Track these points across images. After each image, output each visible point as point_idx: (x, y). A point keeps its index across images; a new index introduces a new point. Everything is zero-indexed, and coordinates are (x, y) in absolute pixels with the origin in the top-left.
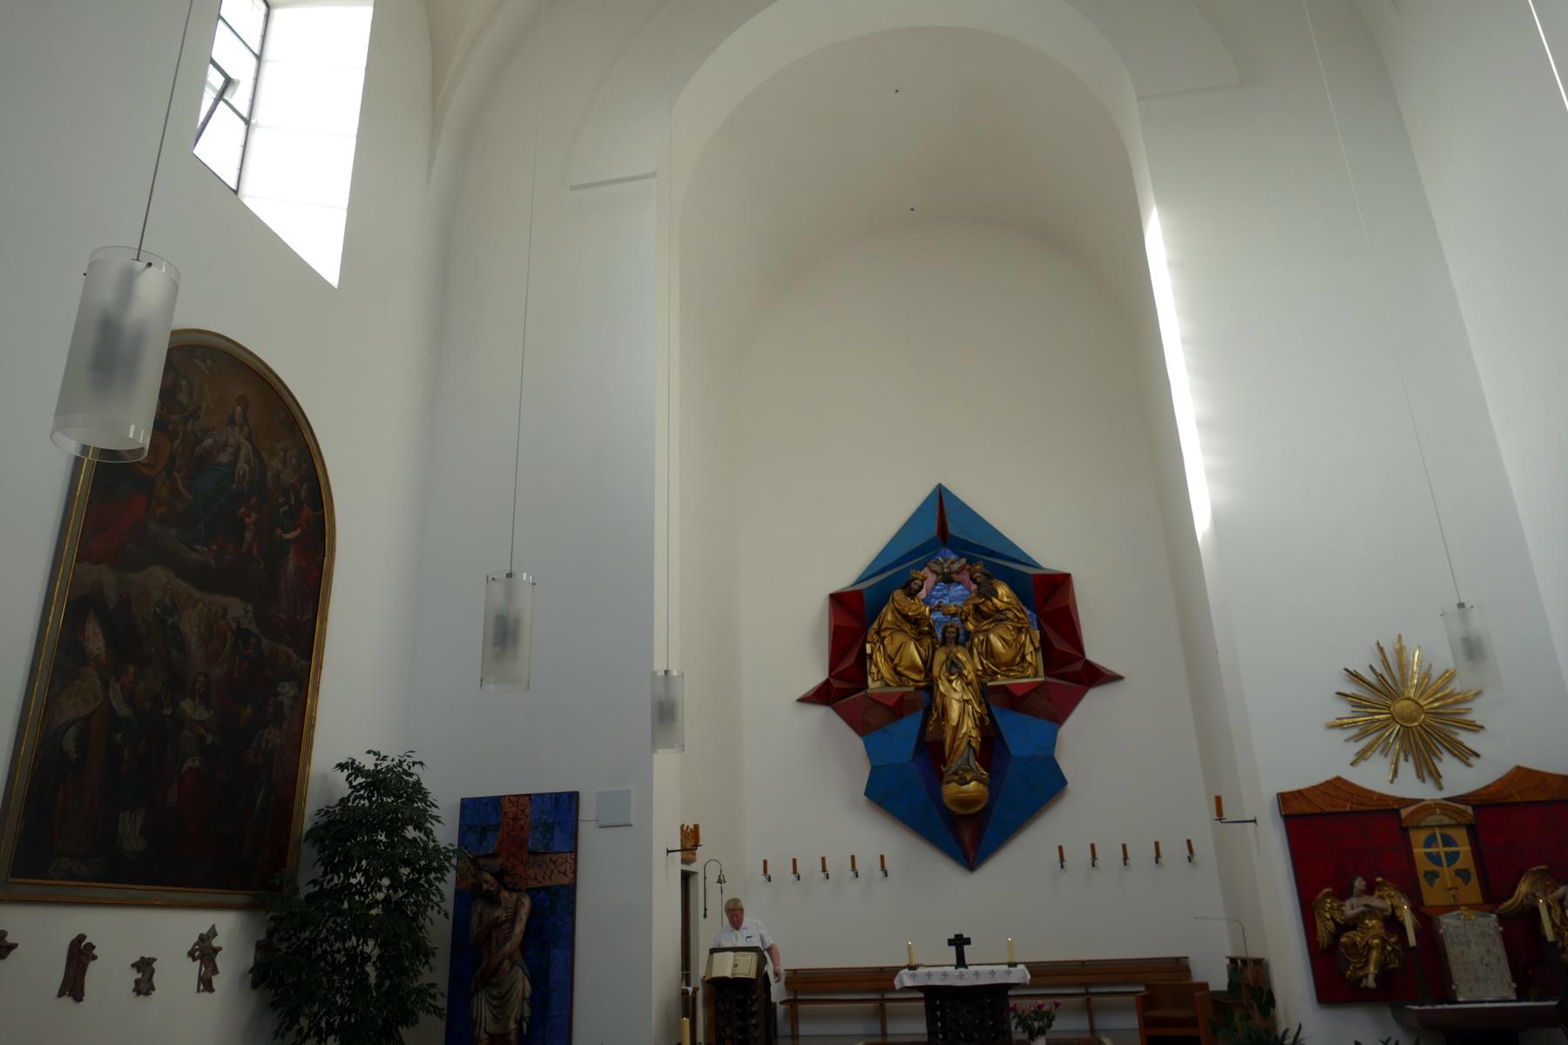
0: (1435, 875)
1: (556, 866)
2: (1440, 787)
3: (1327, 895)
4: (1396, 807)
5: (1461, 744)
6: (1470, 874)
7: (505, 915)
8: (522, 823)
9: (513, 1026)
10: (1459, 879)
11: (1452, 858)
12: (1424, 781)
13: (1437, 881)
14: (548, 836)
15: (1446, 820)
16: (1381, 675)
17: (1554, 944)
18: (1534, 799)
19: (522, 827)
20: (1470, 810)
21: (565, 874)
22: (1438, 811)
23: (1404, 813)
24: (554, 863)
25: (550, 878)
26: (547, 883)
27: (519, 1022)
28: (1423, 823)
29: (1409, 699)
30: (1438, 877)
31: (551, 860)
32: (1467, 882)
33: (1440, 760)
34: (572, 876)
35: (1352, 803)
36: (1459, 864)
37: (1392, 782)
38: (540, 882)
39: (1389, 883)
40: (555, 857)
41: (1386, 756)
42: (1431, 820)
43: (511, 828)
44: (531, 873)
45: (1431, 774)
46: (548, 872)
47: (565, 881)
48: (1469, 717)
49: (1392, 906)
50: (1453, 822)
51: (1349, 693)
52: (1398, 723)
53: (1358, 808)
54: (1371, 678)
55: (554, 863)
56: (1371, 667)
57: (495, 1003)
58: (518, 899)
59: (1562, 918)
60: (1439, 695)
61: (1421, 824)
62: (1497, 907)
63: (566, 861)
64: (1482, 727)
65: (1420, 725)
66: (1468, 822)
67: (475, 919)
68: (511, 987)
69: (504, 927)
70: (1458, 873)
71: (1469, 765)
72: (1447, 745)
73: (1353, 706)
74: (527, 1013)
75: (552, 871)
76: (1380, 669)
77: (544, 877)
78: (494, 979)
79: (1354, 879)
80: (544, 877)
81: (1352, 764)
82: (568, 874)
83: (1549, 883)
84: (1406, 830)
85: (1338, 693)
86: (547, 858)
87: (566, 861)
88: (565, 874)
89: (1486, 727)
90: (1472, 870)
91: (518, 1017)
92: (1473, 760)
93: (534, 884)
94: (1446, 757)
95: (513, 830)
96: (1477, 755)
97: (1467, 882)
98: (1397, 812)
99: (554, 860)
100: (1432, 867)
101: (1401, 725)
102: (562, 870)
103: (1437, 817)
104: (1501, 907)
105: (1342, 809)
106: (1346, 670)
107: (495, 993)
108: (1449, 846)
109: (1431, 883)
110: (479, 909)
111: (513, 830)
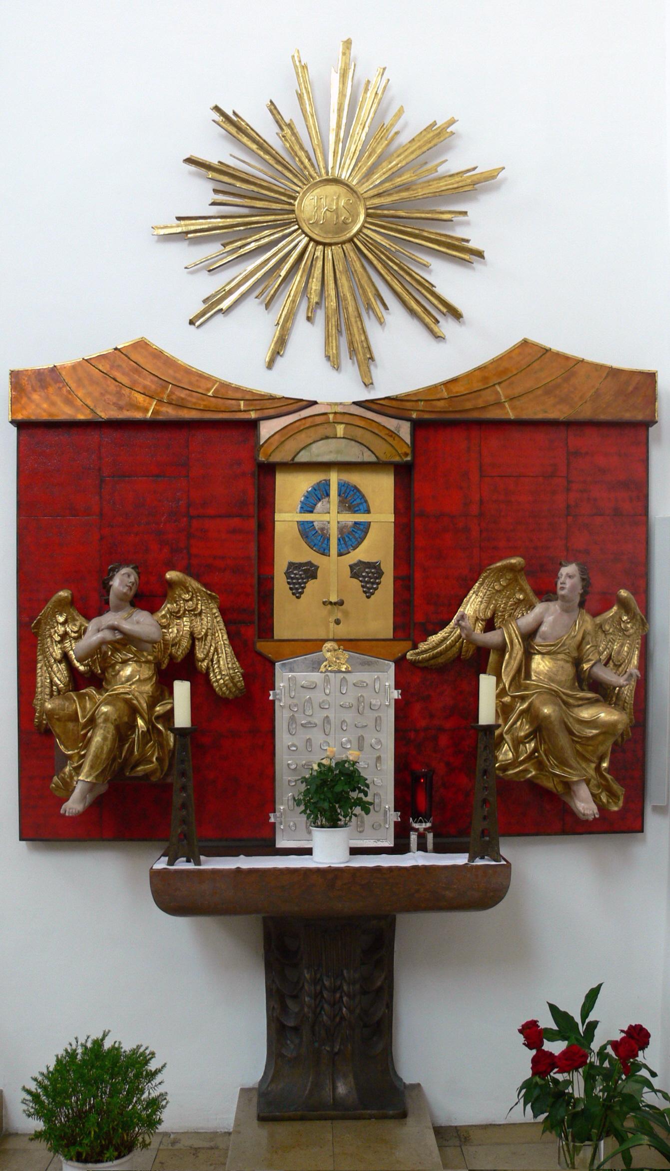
0: (310, 571)
2: (368, 384)
3: (61, 606)
4: (253, 415)
5: (429, 289)
6: (380, 574)
10: (356, 583)
11: (359, 531)
12: (337, 367)
13: (311, 585)
15: (354, 453)
16: (290, 126)
17: (489, 729)
18: (540, 416)
20: (405, 430)
22: (340, 430)
23: (267, 429)
28: (303, 457)
29: (336, 181)
30: (314, 576)
32: (369, 593)
33: (381, 322)
35: (160, 401)
36: (361, 554)
37: (270, 365)
39: (195, 584)
41: (267, 306)
42: (321, 451)
45: (353, 351)
48: (460, 232)
49: (193, 637)
50: (368, 457)
51: (213, 160)
52: (307, 235)
53: (170, 413)
54: (268, 131)
56: (273, 108)
59: (519, 671)
60: (398, 181)
61: (297, 460)
62: (415, 647)
64: (480, 254)
65: (351, 240)
66: (397, 459)
70: (357, 570)
71: (438, 337)
72: (399, 289)
73: (216, 191)
76: (289, 112)
79: (114, 570)
81: (192, 322)
83: (521, 597)
84: (268, 470)
85: (190, 161)
89: (485, 255)
90: (388, 568)
92: (447, 326)
94: (396, 315)
96: (456, 314)
97: (369, 593)
98: (253, 425)
100: (307, 555)
101: (311, 239)
103: (332, 444)
104: (423, 646)
105: (139, 415)
106: (217, 109)
108: (353, 509)
109: (297, 590)
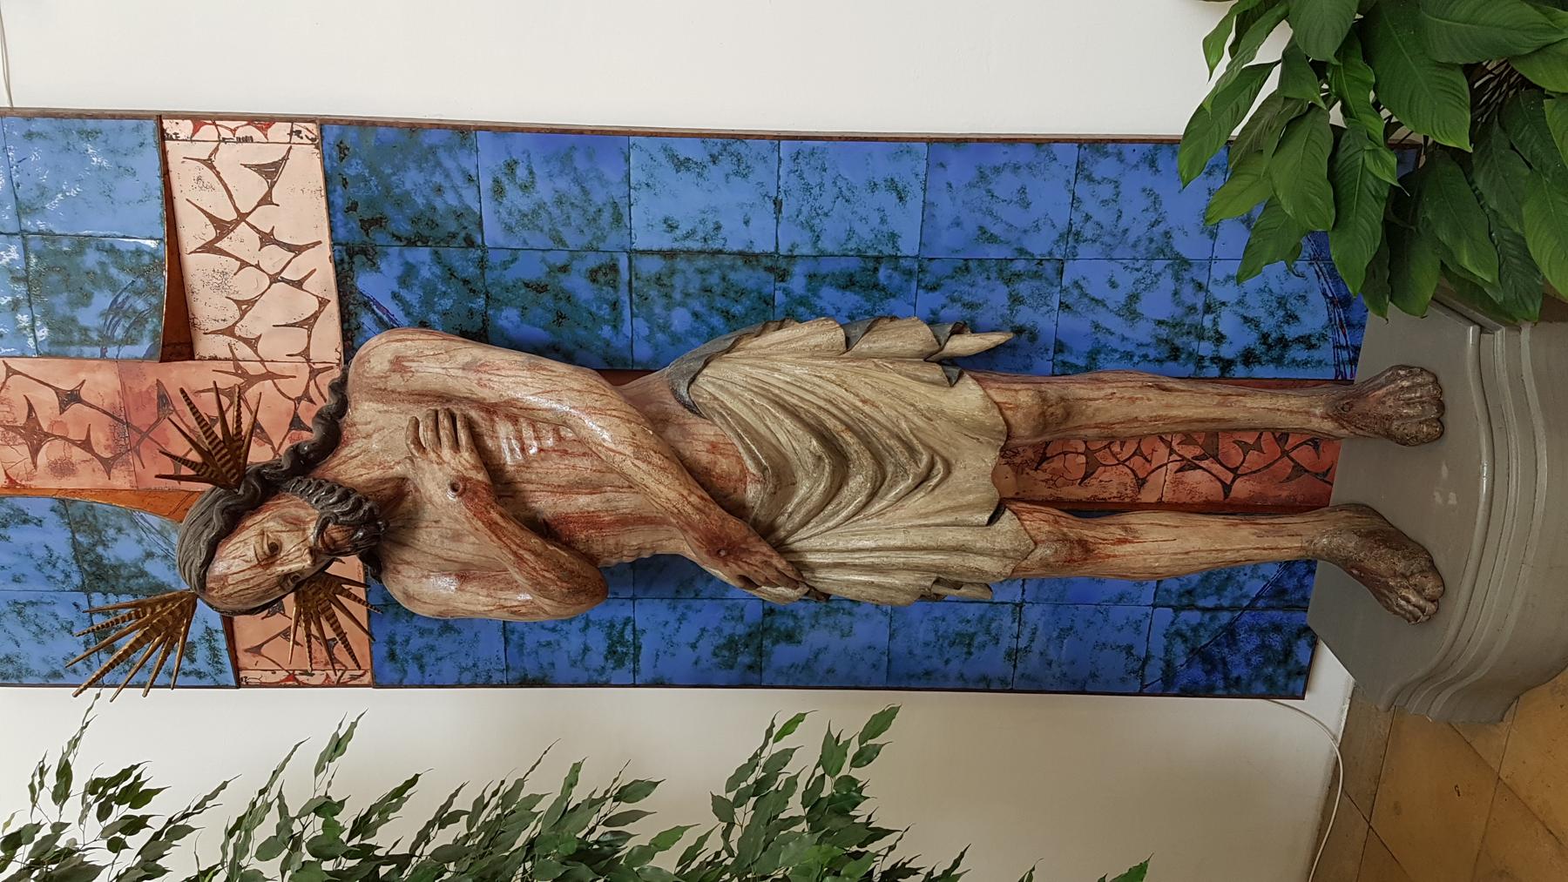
1: (242, 217)
7: (446, 453)
8: (46, 402)
9: (968, 397)
14: (91, 259)
19: (70, 398)
21: (271, 172)
24: (223, 228)
25: (297, 250)
26: (320, 266)
27: (956, 367)
31: (209, 248)
34: (280, 131)
38: (323, 303)
40: (194, 231)
43: (77, 454)
44: (279, 348)
46: (273, 258)
47: (306, 168)
55: (223, 228)
57: (858, 484)
58: (383, 394)
63: (209, 163)
67: (474, 601)
68: (793, 412)
69: (509, 460)
74: (913, 336)
75: (267, 239)
77: (298, 284)
78: (753, 493)
80: (298, 284)
82: (270, 155)
86: (197, 266)
87: (209, 163)
88: (271, 172)
91: (936, 372)
93: (328, 334)
95: (86, 445)
99: (211, 233)
102: (259, 186)
107: (808, 488)
110: (445, 586)
111: (86, 445)
